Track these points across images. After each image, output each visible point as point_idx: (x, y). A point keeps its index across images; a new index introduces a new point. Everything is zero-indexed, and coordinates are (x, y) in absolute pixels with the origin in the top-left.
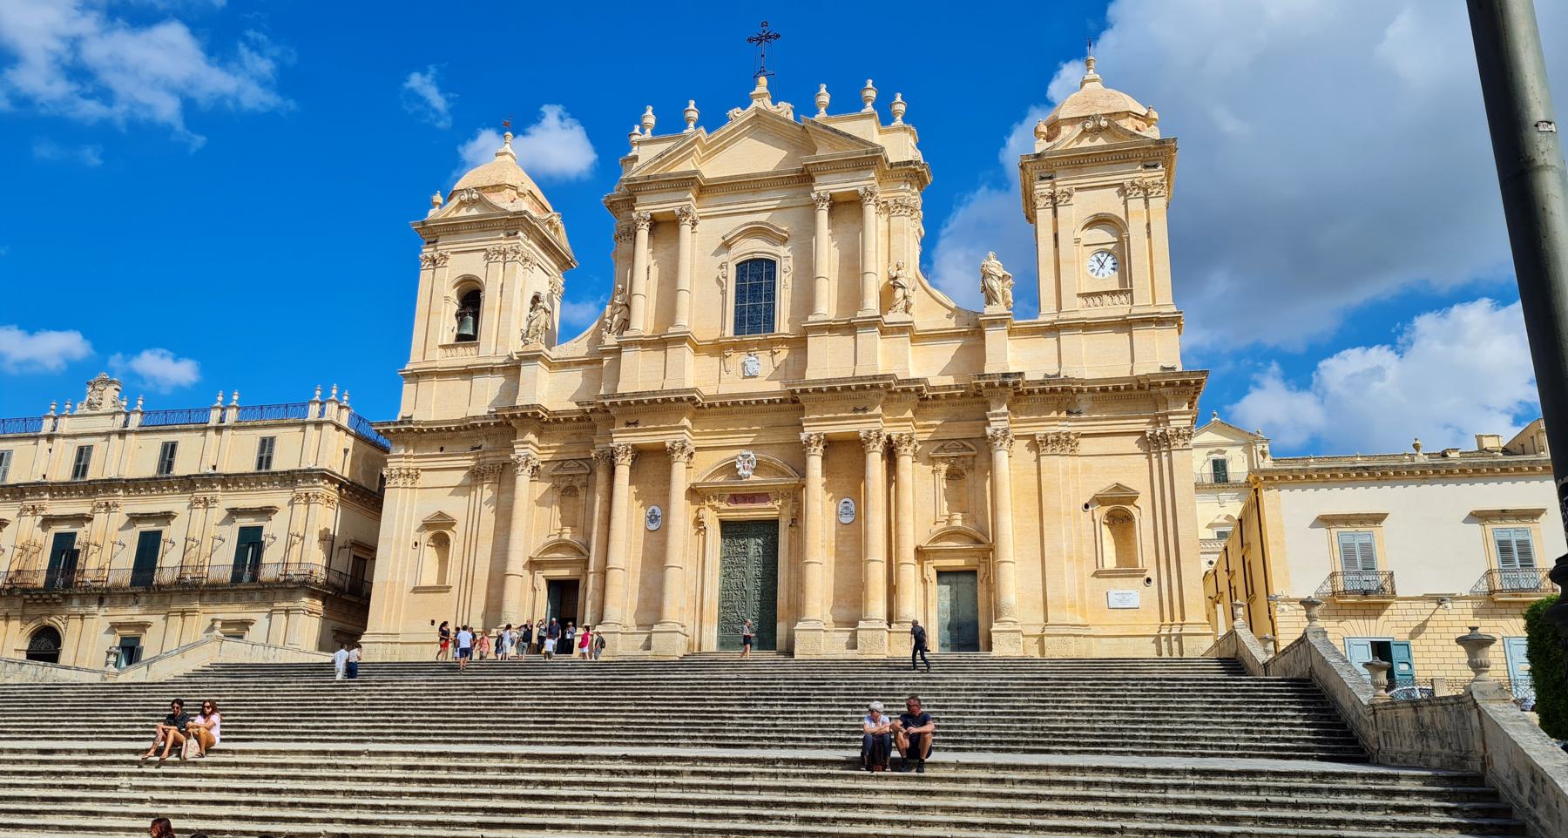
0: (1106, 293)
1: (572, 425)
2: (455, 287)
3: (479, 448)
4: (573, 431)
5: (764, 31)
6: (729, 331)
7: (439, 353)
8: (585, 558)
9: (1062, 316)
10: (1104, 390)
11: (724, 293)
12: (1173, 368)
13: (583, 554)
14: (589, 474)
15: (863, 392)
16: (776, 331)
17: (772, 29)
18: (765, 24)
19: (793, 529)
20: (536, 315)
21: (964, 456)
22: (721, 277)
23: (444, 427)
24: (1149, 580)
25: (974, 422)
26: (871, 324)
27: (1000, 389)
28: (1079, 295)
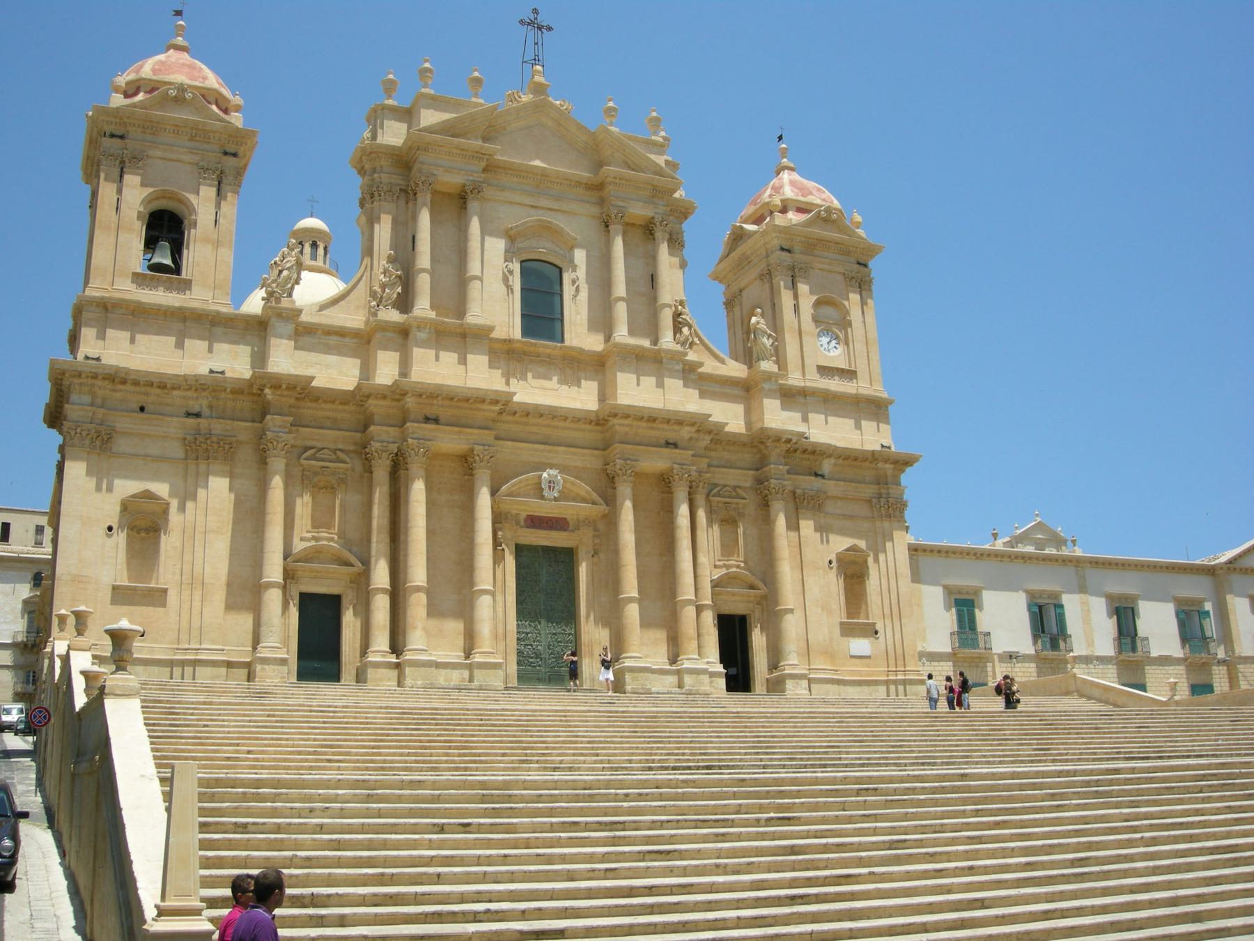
0: (837, 369)
1: (328, 406)
2: (149, 202)
3: (198, 415)
4: (328, 414)
5: (536, 19)
6: (517, 333)
7: (132, 287)
8: (355, 569)
9: (809, 384)
10: (847, 458)
11: (510, 288)
12: (889, 448)
13: (351, 565)
14: (347, 470)
15: (676, 427)
16: (567, 343)
17: (543, 19)
18: (535, 11)
19: (596, 559)
20: (288, 265)
21: (737, 503)
22: (506, 270)
23: (155, 380)
24: (876, 633)
25: (746, 472)
26: (677, 357)
27: (782, 445)
28: (817, 366)
